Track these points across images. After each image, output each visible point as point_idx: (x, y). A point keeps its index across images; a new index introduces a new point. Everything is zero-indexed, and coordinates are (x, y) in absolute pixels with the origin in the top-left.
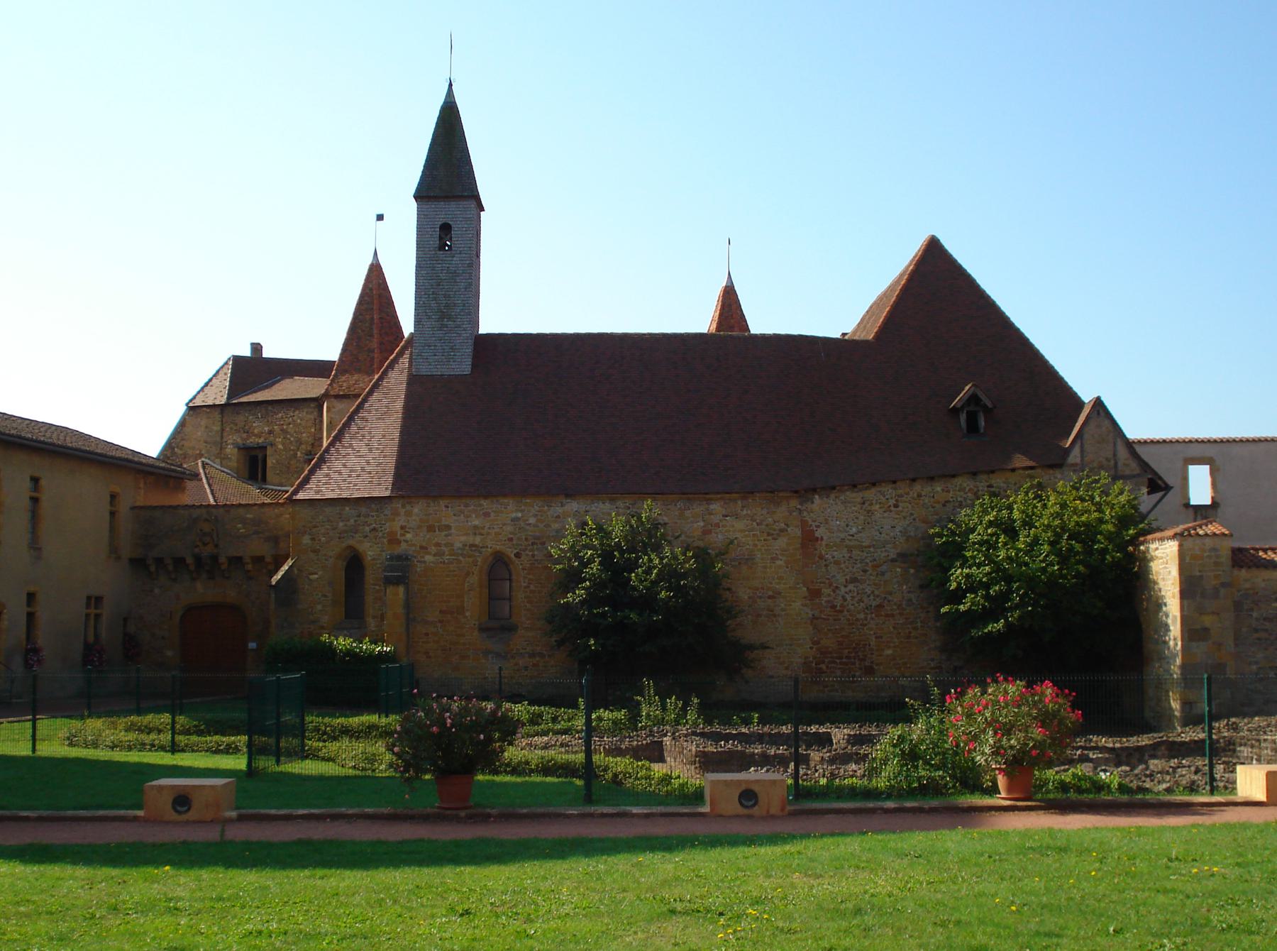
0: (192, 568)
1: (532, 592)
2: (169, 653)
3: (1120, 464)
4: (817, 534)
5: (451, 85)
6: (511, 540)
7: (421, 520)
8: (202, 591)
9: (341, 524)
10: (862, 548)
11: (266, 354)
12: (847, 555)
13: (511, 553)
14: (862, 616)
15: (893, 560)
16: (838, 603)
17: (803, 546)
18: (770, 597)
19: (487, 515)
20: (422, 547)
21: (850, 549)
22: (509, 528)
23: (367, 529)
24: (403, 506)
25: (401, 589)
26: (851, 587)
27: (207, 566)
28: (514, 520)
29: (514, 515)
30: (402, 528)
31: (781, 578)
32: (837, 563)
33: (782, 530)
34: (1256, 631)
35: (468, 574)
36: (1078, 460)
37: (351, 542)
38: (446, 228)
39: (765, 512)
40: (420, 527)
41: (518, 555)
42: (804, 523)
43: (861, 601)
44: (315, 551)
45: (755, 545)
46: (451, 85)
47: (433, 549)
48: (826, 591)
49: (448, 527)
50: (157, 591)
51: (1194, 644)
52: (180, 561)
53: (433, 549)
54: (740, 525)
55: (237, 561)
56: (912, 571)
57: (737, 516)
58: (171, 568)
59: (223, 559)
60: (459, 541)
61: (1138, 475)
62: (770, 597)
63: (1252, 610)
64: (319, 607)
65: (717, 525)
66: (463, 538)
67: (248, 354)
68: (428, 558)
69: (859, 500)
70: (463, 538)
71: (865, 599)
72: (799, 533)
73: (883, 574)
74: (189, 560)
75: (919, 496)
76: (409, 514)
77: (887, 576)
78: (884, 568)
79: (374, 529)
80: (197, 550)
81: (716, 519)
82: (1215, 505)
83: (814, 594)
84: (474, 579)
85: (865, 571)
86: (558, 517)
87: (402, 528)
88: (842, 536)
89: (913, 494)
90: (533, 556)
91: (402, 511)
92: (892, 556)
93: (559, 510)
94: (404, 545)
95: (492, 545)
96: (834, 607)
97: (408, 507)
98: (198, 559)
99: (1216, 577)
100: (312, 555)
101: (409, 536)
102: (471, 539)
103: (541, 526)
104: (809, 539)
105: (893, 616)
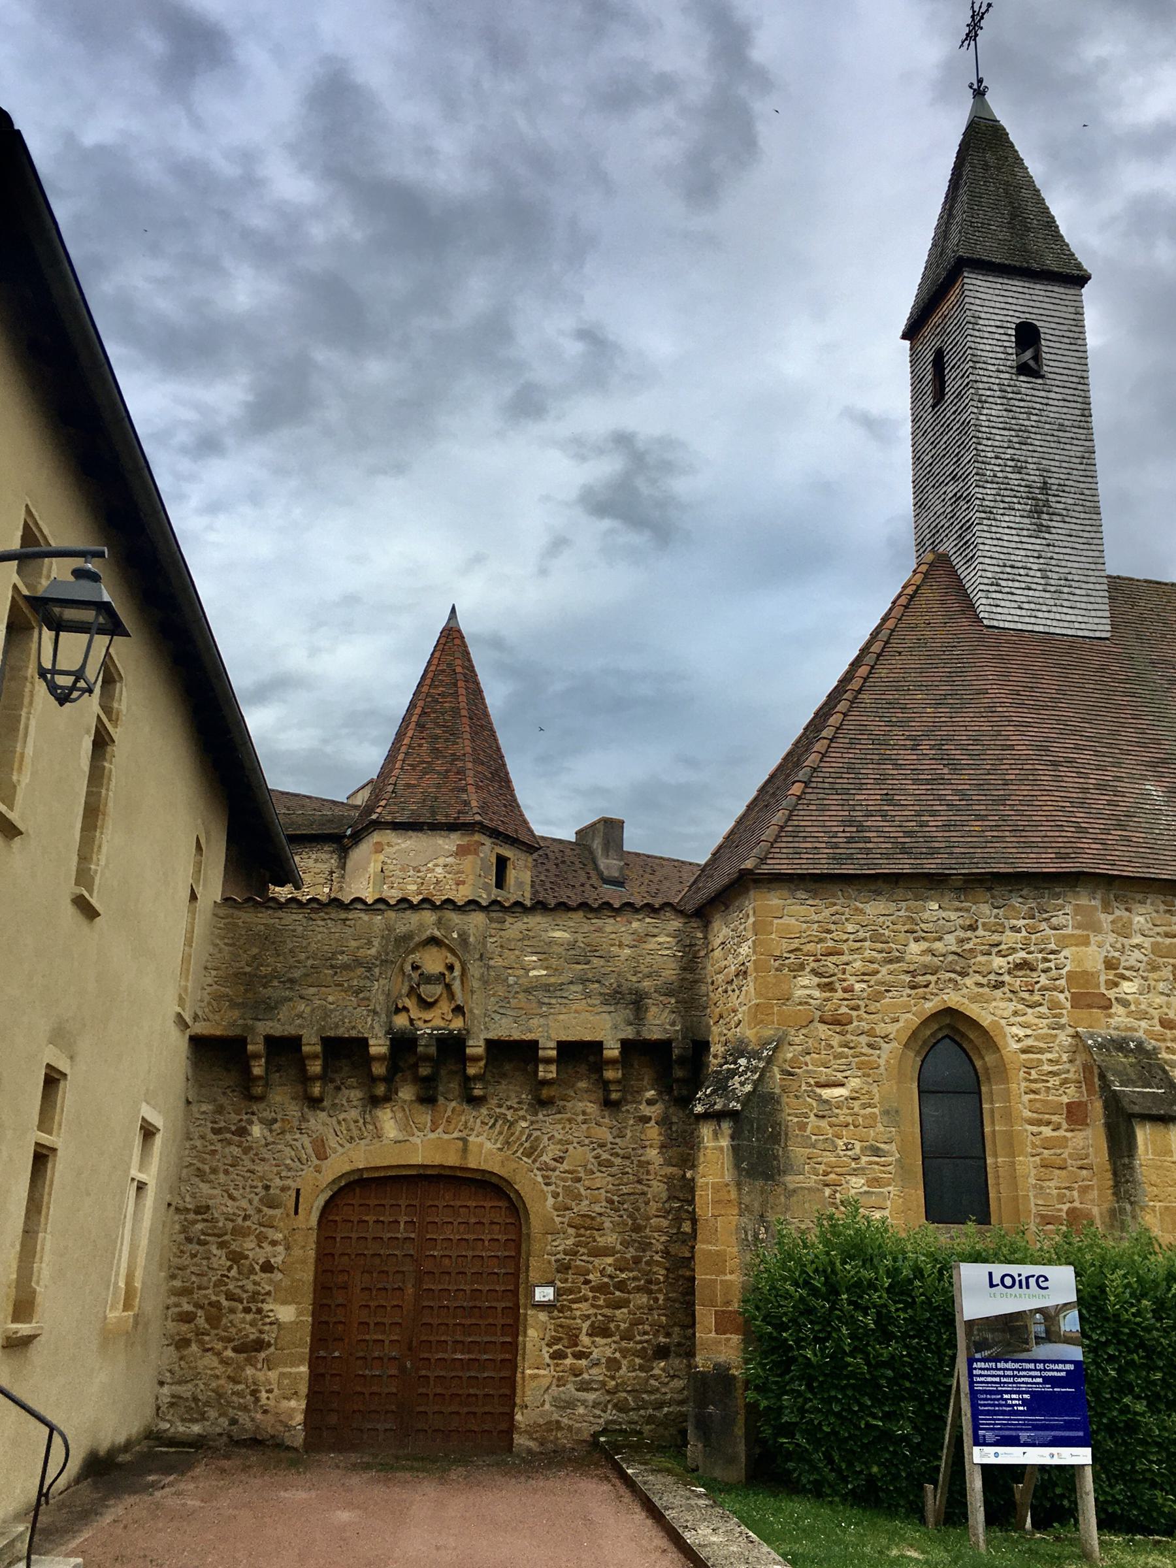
0: (379, 1069)
2: (286, 1313)
8: (402, 1136)
9: (914, 948)
23: (998, 962)
24: (1107, 908)
37: (952, 999)
44: (838, 1022)
50: (256, 1130)
55: (514, 1055)
58: (315, 1068)
59: (476, 1047)
64: (857, 1184)
74: (378, 1046)
76: (1124, 930)
79: (1024, 965)
80: (401, 1021)
87: (1110, 965)
91: (1105, 919)
94: (1120, 1017)
98: (402, 1043)
100: (823, 1030)
101: (1127, 987)
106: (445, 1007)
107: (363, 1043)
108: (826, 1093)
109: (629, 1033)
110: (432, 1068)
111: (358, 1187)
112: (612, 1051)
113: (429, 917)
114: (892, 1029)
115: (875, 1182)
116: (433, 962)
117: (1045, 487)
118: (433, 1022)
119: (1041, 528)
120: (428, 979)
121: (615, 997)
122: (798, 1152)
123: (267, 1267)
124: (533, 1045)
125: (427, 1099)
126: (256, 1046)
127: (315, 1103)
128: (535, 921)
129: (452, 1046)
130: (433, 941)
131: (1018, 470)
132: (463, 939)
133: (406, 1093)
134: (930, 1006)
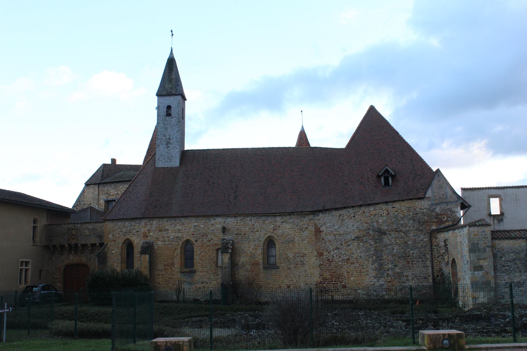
1: (202, 256)
2: (59, 285)
3: (448, 197)
4: (321, 229)
5: (172, 50)
6: (193, 234)
7: (156, 227)
8: (73, 259)
10: (340, 235)
11: (118, 163)
12: (334, 238)
13: (193, 240)
14: (341, 263)
15: (353, 240)
16: (330, 258)
17: (316, 235)
18: (302, 256)
19: (183, 224)
20: (157, 238)
21: (335, 235)
22: (192, 230)
24: (149, 221)
25: (147, 256)
26: (336, 251)
27: (74, 248)
28: (196, 226)
29: (194, 224)
30: (149, 230)
31: (306, 248)
32: (330, 241)
33: (306, 228)
34: (504, 266)
35: (176, 249)
36: (430, 196)
37: (128, 237)
38: (169, 107)
39: (298, 220)
40: (156, 230)
41: (196, 241)
42: (316, 225)
43: (340, 257)
44: (114, 241)
45: (295, 235)
46: (172, 50)
47: (161, 239)
48: (325, 253)
49: (168, 230)
50: (54, 259)
51: (476, 272)
52: (62, 247)
53: (161, 239)
54: (288, 226)
55: (84, 246)
56: (361, 244)
57: (287, 222)
59: (79, 245)
60: (172, 235)
61: (457, 201)
62: (302, 256)
63: (502, 257)
65: (279, 227)
66: (173, 234)
67: (110, 163)
68: (159, 243)
69: (338, 214)
70: (173, 234)
71: (342, 256)
72: (314, 229)
73: (349, 246)
75: (364, 212)
76: (152, 225)
77: (351, 247)
78: (349, 243)
79: (137, 231)
80: (70, 242)
81: (278, 224)
82: (502, 214)
83: (321, 254)
84: (178, 251)
85: (342, 245)
86: (213, 224)
88: (332, 230)
89: (361, 211)
90: (203, 241)
91: (148, 223)
92: (353, 238)
93: (213, 222)
94: (149, 238)
95: (186, 237)
96: (329, 260)
97: (151, 222)
98: (70, 245)
99: (485, 243)
100: (113, 242)
101: (151, 234)
102: (177, 235)
103: (206, 228)
104: (318, 231)
105: (354, 263)
106: (76, 239)
107: (64, 245)
108: (113, 252)
109: (100, 242)
110: (74, 248)
111: (67, 267)
112: (98, 245)
113: (72, 225)
114: (120, 242)
115: (118, 264)
116: (74, 232)
117: (169, 139)
118: (73, 242)
119: (168, 147)
120: (73, 235)
121: (98, 236)
122: (109, 260)
123: (57, 278)
124: (87, 244)
125: (76, 253)
126: (51, 247)
127: (61, 254)
128: (87, 225)
129: (76, 245)
130: (73, 229)
131: (165, 136)
132: (77, 228)
133: (73, 252)
134: (126, 238)
